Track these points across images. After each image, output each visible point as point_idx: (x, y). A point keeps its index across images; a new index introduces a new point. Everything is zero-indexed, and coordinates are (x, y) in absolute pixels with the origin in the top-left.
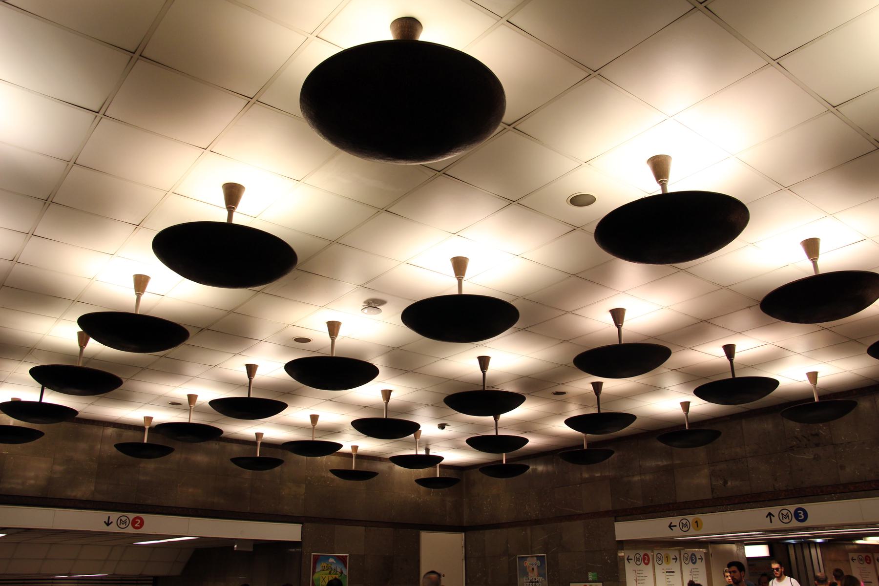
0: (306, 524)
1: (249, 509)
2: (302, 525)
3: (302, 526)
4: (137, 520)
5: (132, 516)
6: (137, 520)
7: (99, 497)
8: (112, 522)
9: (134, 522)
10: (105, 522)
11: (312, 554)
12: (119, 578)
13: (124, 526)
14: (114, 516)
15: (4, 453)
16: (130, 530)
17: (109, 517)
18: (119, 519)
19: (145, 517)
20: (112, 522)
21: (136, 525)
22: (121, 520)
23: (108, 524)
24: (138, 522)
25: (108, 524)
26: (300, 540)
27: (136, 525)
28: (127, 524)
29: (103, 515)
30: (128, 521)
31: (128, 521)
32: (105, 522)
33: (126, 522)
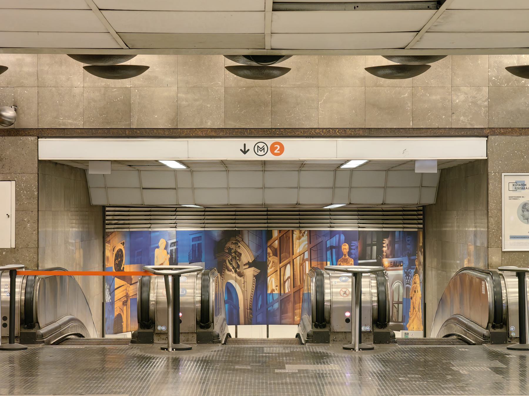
0: (492, 138)
1: (411, 124)
2: (487, 139)
3: (487, 140)
4: (275, 146)
5: (270, 141)
6: (275, 146)
7: (232, 124)
8: (248, 150)
9: (273, 149)
10: (241, 150)
11: (503, 174)
12: (401, 209)
13: (262, 153)
14: (250, 143)
15: (128, 86)
16: (269, 157)
17: (245, 145)
18: (256, 146)
19: (283, 141)
20: (248, 150)
21: (276, 152)
22: (258, 147)
23: (245, 152)
24: (277, 147)
25: (245, 152)
26: (486, 158)
27: (276, 152)
28: (266, 151)
29: (237, 143)
30: (265, 147)
31: (265, 147)
32: (241, 150)
33: (264, 149)
